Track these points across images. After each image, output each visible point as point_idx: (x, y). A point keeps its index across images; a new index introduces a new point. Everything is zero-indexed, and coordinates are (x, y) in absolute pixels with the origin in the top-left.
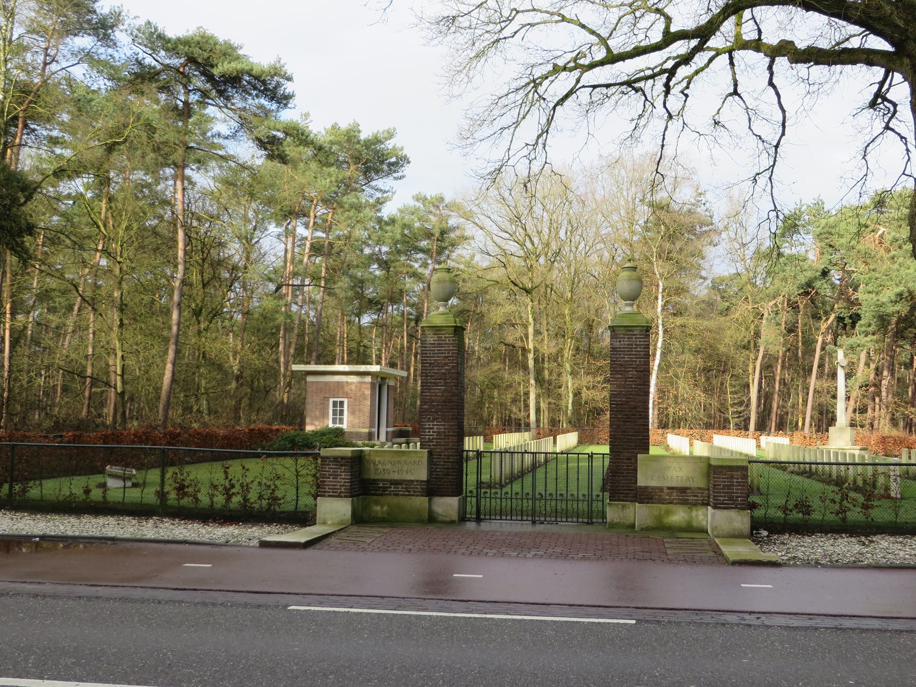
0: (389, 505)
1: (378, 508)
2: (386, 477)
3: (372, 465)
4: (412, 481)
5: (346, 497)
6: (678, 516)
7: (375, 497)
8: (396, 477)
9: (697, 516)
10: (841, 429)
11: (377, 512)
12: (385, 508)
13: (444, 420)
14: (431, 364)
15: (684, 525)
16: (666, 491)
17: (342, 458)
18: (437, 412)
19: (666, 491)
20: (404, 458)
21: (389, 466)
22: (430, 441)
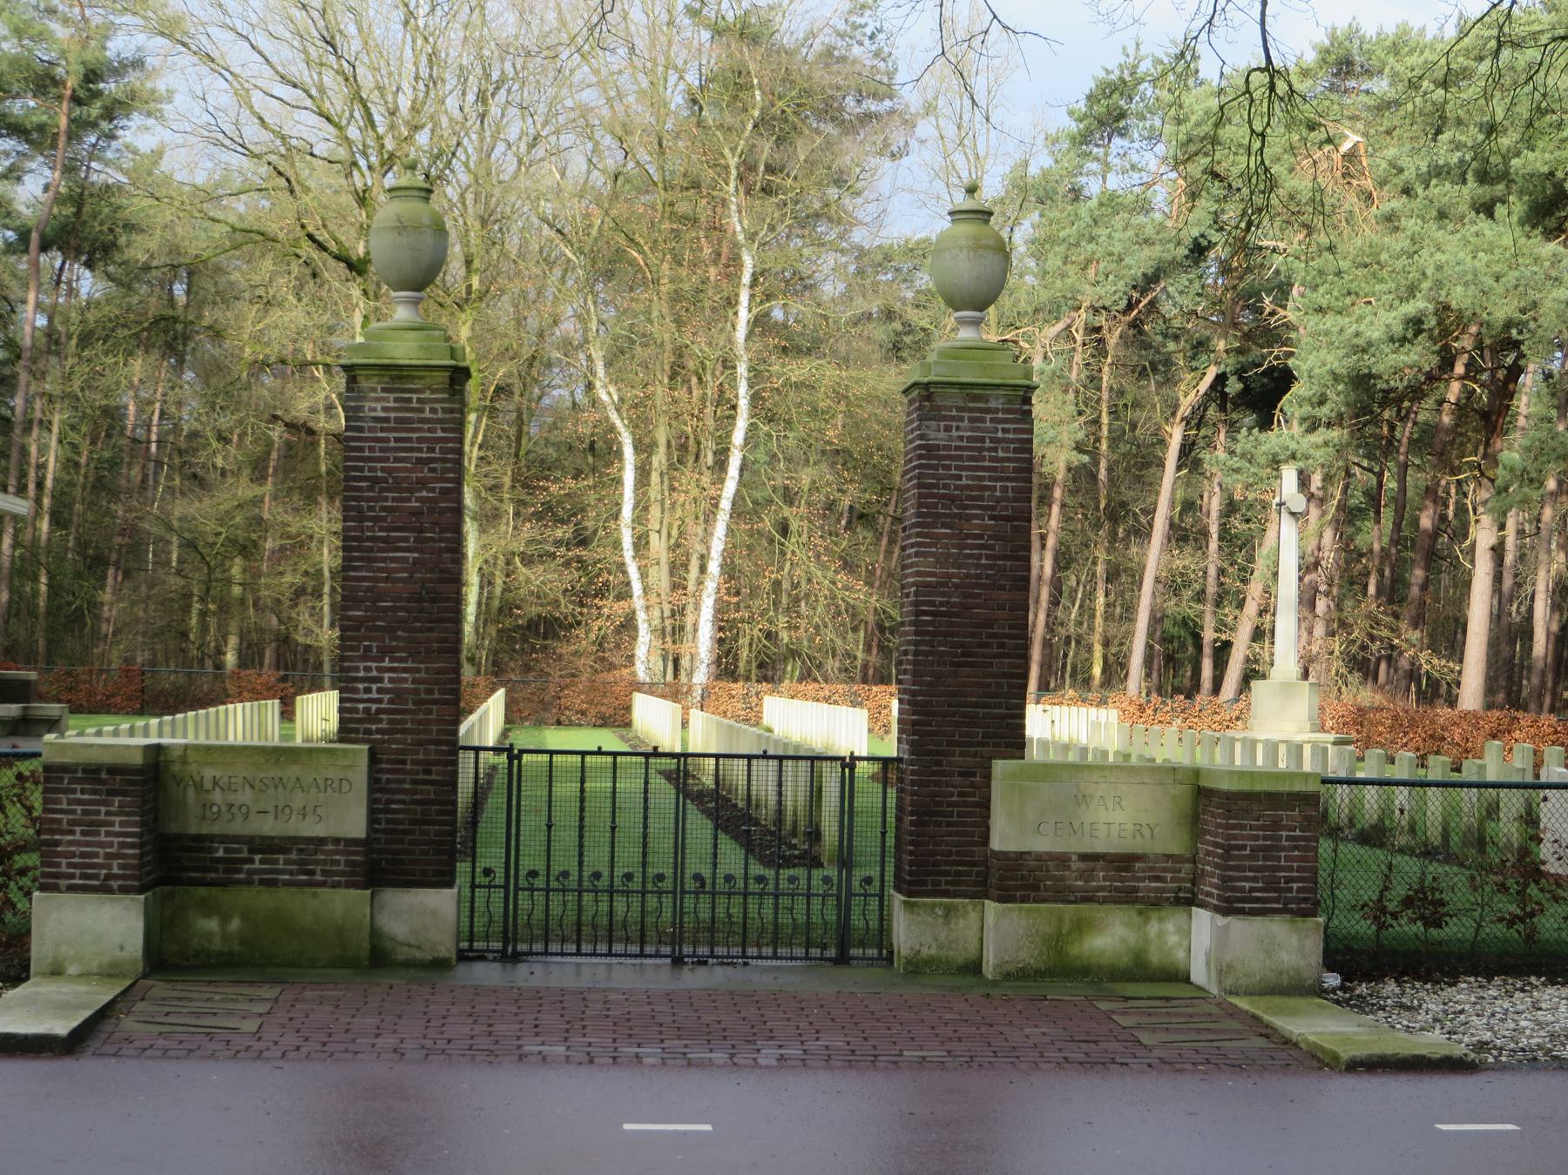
0: (245, 917)
1: (213, 925)
2: (237, 827)
3: (191, 792)
4: (321, 841)
5: (125, 890)
6: (1111, 936)
7: (202, 891)
8: (268, 827)
9: (1161, 934)
10: (1286, 687)
11: (209, 936)
12: (235, 924)
13: (414, 655)
14: (375, 481)
15: (1126, 960)
16: (1076, 865)
17: (114, 770)
18: (391, 630)
19: (1076, 865)
20: (293, 771)
21: (245, 796)
22: (370, 717)
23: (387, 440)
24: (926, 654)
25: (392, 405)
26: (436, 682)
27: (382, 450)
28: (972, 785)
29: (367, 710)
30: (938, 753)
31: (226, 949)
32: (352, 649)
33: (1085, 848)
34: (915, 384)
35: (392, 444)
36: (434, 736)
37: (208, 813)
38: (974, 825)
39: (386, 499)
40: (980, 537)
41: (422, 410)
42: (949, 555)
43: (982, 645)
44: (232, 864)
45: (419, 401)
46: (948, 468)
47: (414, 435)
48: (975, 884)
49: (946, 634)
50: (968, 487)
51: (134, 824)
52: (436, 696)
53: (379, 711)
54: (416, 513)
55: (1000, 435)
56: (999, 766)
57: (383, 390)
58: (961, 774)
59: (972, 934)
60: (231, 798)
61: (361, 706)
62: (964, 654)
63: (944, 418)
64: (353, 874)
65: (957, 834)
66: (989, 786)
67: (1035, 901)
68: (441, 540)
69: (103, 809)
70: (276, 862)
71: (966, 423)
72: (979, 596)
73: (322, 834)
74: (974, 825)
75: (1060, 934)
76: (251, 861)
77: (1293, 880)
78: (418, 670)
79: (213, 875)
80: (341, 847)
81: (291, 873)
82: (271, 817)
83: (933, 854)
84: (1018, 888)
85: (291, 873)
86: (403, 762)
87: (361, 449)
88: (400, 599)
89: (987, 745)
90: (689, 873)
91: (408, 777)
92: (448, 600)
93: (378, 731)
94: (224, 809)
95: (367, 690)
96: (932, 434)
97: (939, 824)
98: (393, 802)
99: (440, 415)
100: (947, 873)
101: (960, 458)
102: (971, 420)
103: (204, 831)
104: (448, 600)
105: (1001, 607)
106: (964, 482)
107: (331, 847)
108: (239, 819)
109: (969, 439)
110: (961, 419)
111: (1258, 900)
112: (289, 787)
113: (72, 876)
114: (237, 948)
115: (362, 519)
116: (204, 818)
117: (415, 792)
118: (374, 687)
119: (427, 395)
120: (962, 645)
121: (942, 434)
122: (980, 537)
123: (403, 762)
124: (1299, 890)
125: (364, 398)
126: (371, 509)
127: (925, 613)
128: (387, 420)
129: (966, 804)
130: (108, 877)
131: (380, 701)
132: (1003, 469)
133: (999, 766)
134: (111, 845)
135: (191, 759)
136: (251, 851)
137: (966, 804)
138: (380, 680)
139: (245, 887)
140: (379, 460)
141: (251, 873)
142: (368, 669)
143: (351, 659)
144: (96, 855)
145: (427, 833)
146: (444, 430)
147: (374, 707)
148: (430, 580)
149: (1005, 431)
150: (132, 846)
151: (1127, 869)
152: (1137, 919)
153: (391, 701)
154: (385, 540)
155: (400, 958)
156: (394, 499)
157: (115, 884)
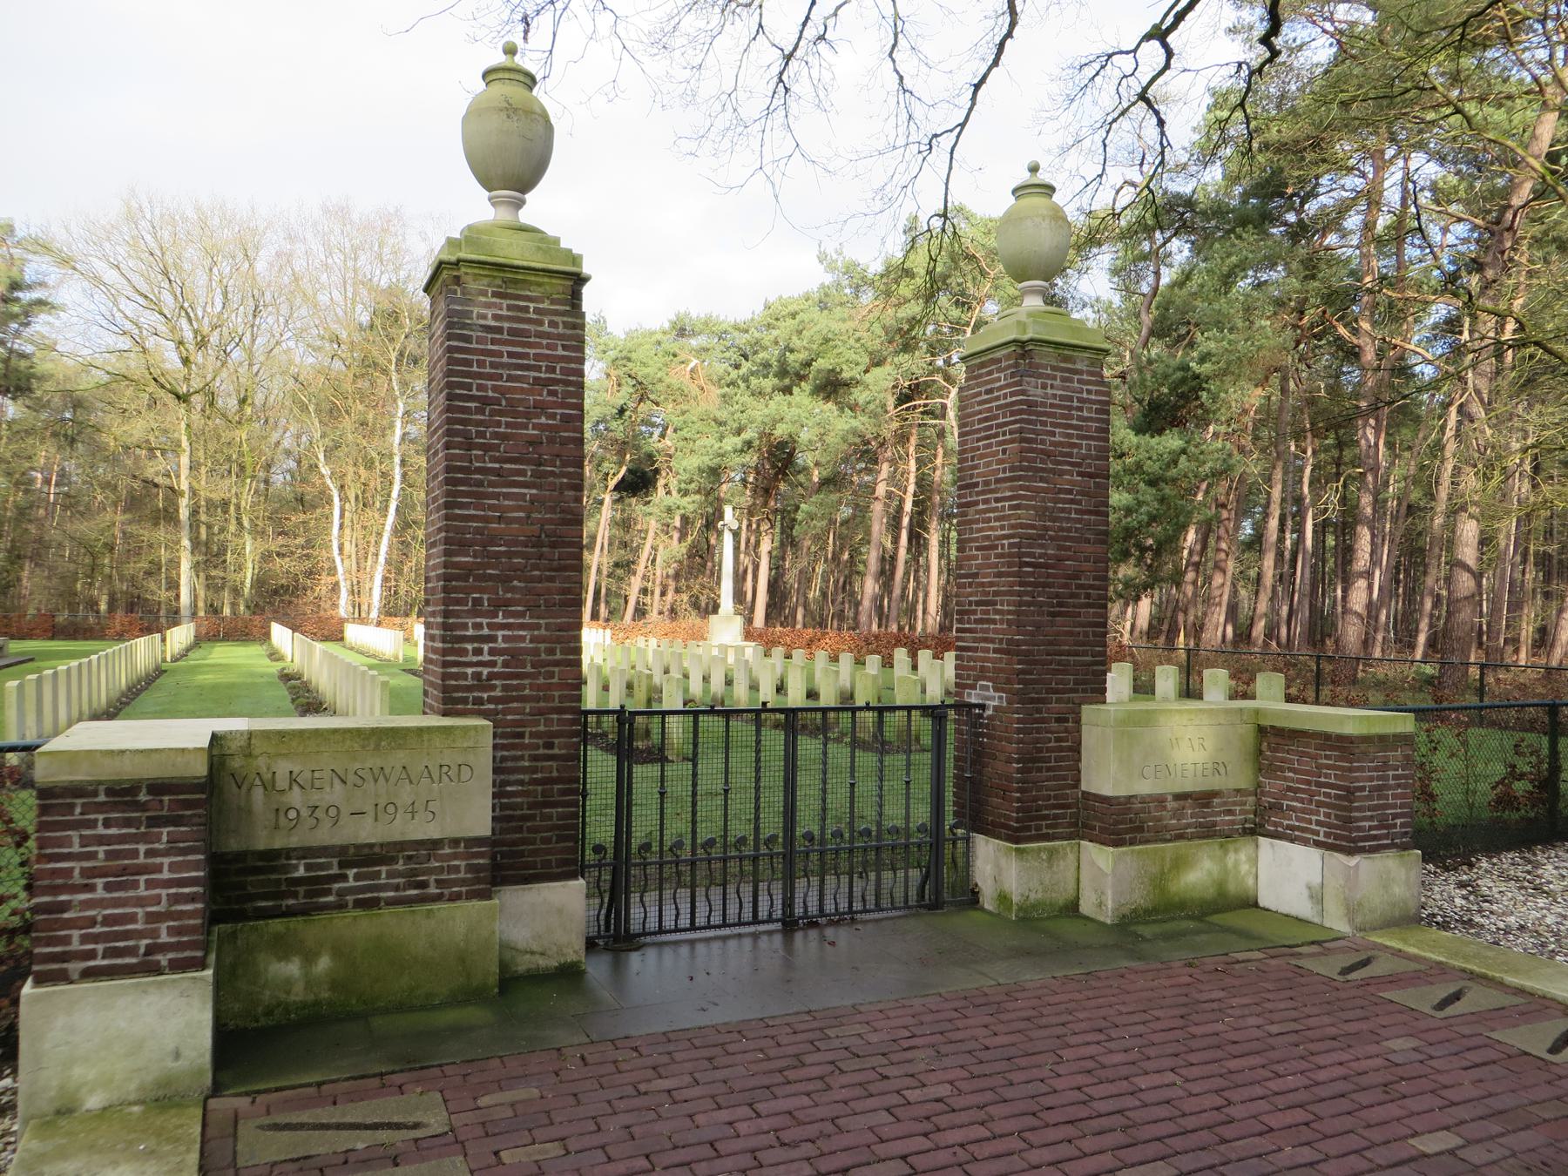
0: (337, 953)
1: (292, 968)
2: (325, 836)
3: (258, 794)
4: (435, 844)
5: (178, 966)
6: (1201, 871)
7: (277, 925)
8: (367, 832)
9: (1237, 864)
10: (728, 618)
11: (288, 982)
12: (324, 963)
13: (532, 608)
14: (485, 401)
15: (1211, 893)
16: (1171, 804)
17: (158, 788)
18: (505, 580)
19: (1171, 804)
20: (399, 757)
21: (335, 794)
22: (482, 684)
23: (500, 354)
24: (1029, 604)
25: (505, 313)
26: (558, 640)
27: (493, 365)
28: (1066, 730)
29: (477, 676)
30: (1039, 701)
31: (311, 997)
32: (458, 602)
33: (1178, 790)
34: (1014, 341)
35: (505, 359)
36: (556, 704)
37: (282, 819)
38: (1068, 768)
39: (499, 424)
40: (1070, 492)
41: (541, 323)
42: (1047, 508)
43: (1072, 596)
44: (317, 885)
45: (537, 311)
46: (1044, 424)
47: (532, 351)
48: (1070, 825)
49: (1045, 585)
50: (1060, 444)
51: (195, 866)
52: (558, 656)
53: (491, 676)
54: (534, 442)
55: (1085, 395)
56: (1087, 710)
57: (495, 294)
58: (1058, 720)
59: (1070, 875)
60: (315, 797)
61: (469, 671)
62: (1060, 605)
63: (1040, 376)
64: (478, 881)
65: (1055, 778)
66: (1079, 731)
67: (1141, 843)
68: (563, 475)
69: (142, 848)
70: (377, 875)
71: (1058, 382)
72: (1069, 548)
73: (436, 836)
74: (1068, 768)
75: (1163, 873)
76: (344, 878)
77: (1395, 816)
78: (538, 627)
79: (291, 902)
80: (461, 849)
81: (397, 888)
82: (368, 820)
83: (1035, 799)
84: (1127, 831)
85: (397, 888)
86: (521, 735)
87: (468, 363)
88: (516, 543)
89: (1076, 691)
90: (799, 831)
91: (527, 753)
92: (571, 544)
93: (491, 700)
94: (305, 813)
95: (478, 652)
96: (1032, 391)
97: (1040, 770)
98: (509, 783)
99: (561, 330)
100: (1046, 817)
101: (1053, 415)
102: (1064, 380)
103: (277, 845)
104: (571, 544)
105: (1087, 560)
106: (1057, 438)
107: (447, 851)
108: (326, 824)
109: (1062, 398)
110: (1054, 378)
111: (1375, 838)
112: (393, 780)
113: (91, 955)
114: (325, 995)
115: (470, 447)
116: (277, 827)
117: (535, 770)
118: (486, 647)
119: (545, 305)
120: (1057, 596)
121: (1039, 391)
122: (1070, 492)
123: (521, 735)
124: (1402, 825)
125: (469, 302)
126: (481, 435)
127: (1028, 564)
128: (499, 330)
129: (1061, 749)
130: (150, 950)
131: (493, 664)
132: (1088, 429)
133: (1087, 710)
134: (157, 900)
135: (257, 752)
136: (342, 865)
137: (1061, 749)
138: (493, 639)
139: (336, 914)
140: (491, 377)
141: (341, 893)
142: (478, 626)
143: (457, 614)
144: (132, 918)
145: (550, 818)
146: (564, 347)
147: (485, 671)
148: (551, 521)
149: (1089, 392)
150: (192, 898)
151: (1207, 805)
152: (1219, 853)
153: (506, 664)
154: (498, 472)
155: (521, 969)
156: (508, 425)
157: (163, 959)
